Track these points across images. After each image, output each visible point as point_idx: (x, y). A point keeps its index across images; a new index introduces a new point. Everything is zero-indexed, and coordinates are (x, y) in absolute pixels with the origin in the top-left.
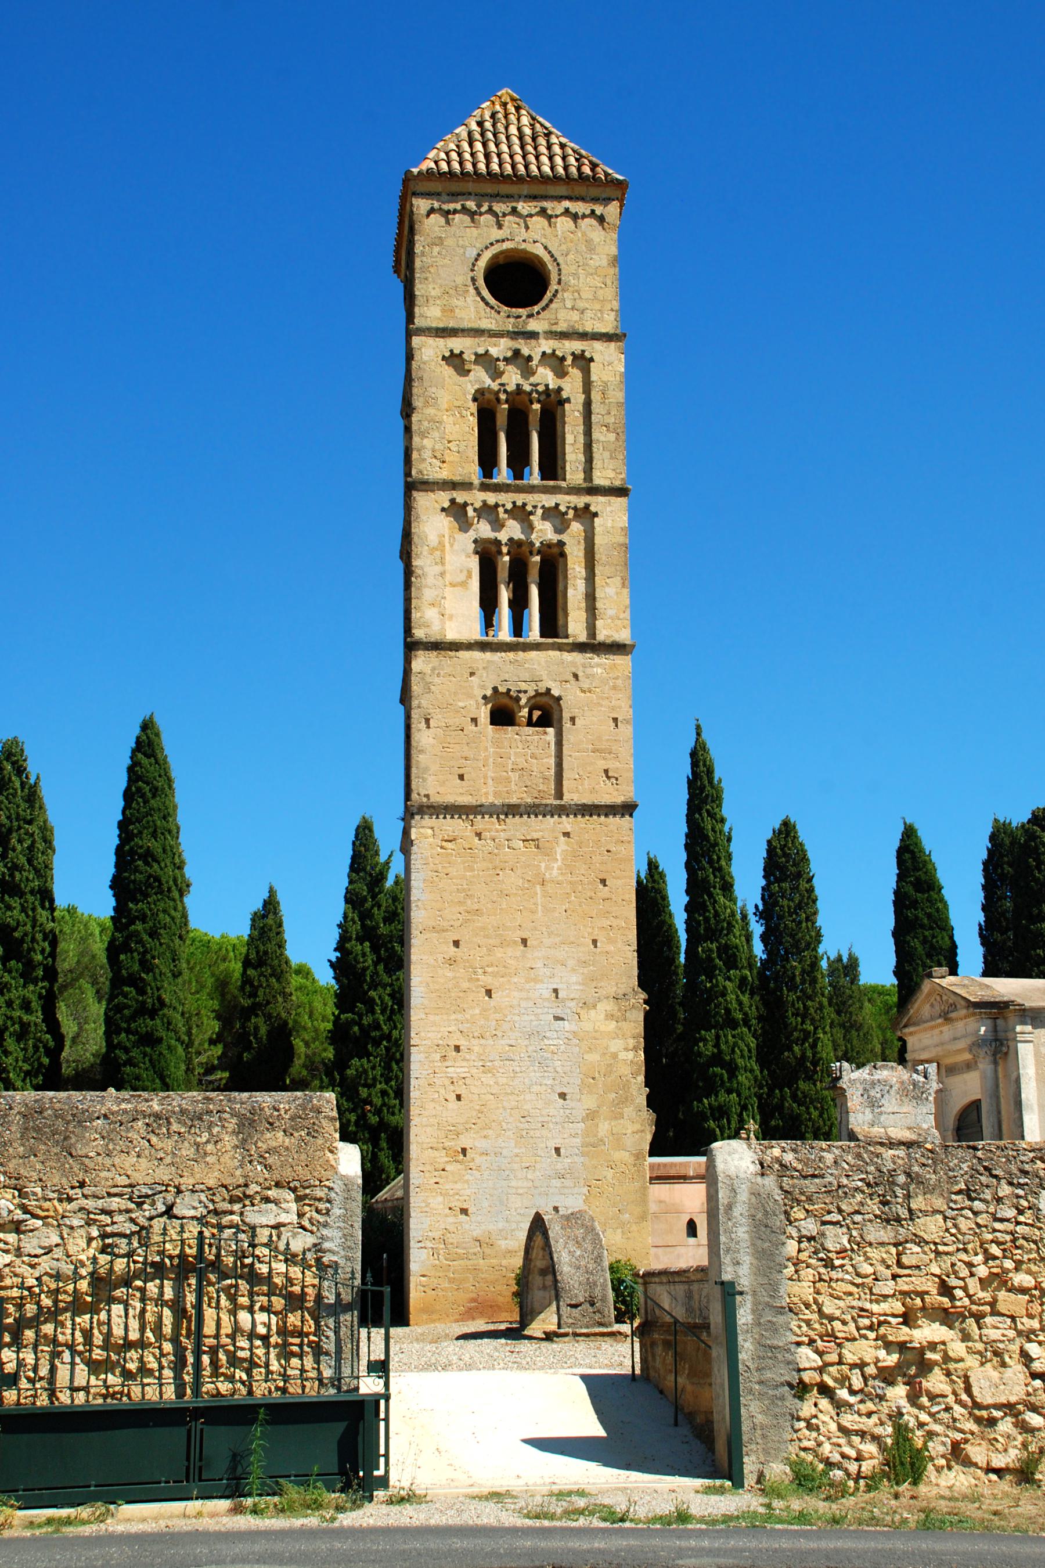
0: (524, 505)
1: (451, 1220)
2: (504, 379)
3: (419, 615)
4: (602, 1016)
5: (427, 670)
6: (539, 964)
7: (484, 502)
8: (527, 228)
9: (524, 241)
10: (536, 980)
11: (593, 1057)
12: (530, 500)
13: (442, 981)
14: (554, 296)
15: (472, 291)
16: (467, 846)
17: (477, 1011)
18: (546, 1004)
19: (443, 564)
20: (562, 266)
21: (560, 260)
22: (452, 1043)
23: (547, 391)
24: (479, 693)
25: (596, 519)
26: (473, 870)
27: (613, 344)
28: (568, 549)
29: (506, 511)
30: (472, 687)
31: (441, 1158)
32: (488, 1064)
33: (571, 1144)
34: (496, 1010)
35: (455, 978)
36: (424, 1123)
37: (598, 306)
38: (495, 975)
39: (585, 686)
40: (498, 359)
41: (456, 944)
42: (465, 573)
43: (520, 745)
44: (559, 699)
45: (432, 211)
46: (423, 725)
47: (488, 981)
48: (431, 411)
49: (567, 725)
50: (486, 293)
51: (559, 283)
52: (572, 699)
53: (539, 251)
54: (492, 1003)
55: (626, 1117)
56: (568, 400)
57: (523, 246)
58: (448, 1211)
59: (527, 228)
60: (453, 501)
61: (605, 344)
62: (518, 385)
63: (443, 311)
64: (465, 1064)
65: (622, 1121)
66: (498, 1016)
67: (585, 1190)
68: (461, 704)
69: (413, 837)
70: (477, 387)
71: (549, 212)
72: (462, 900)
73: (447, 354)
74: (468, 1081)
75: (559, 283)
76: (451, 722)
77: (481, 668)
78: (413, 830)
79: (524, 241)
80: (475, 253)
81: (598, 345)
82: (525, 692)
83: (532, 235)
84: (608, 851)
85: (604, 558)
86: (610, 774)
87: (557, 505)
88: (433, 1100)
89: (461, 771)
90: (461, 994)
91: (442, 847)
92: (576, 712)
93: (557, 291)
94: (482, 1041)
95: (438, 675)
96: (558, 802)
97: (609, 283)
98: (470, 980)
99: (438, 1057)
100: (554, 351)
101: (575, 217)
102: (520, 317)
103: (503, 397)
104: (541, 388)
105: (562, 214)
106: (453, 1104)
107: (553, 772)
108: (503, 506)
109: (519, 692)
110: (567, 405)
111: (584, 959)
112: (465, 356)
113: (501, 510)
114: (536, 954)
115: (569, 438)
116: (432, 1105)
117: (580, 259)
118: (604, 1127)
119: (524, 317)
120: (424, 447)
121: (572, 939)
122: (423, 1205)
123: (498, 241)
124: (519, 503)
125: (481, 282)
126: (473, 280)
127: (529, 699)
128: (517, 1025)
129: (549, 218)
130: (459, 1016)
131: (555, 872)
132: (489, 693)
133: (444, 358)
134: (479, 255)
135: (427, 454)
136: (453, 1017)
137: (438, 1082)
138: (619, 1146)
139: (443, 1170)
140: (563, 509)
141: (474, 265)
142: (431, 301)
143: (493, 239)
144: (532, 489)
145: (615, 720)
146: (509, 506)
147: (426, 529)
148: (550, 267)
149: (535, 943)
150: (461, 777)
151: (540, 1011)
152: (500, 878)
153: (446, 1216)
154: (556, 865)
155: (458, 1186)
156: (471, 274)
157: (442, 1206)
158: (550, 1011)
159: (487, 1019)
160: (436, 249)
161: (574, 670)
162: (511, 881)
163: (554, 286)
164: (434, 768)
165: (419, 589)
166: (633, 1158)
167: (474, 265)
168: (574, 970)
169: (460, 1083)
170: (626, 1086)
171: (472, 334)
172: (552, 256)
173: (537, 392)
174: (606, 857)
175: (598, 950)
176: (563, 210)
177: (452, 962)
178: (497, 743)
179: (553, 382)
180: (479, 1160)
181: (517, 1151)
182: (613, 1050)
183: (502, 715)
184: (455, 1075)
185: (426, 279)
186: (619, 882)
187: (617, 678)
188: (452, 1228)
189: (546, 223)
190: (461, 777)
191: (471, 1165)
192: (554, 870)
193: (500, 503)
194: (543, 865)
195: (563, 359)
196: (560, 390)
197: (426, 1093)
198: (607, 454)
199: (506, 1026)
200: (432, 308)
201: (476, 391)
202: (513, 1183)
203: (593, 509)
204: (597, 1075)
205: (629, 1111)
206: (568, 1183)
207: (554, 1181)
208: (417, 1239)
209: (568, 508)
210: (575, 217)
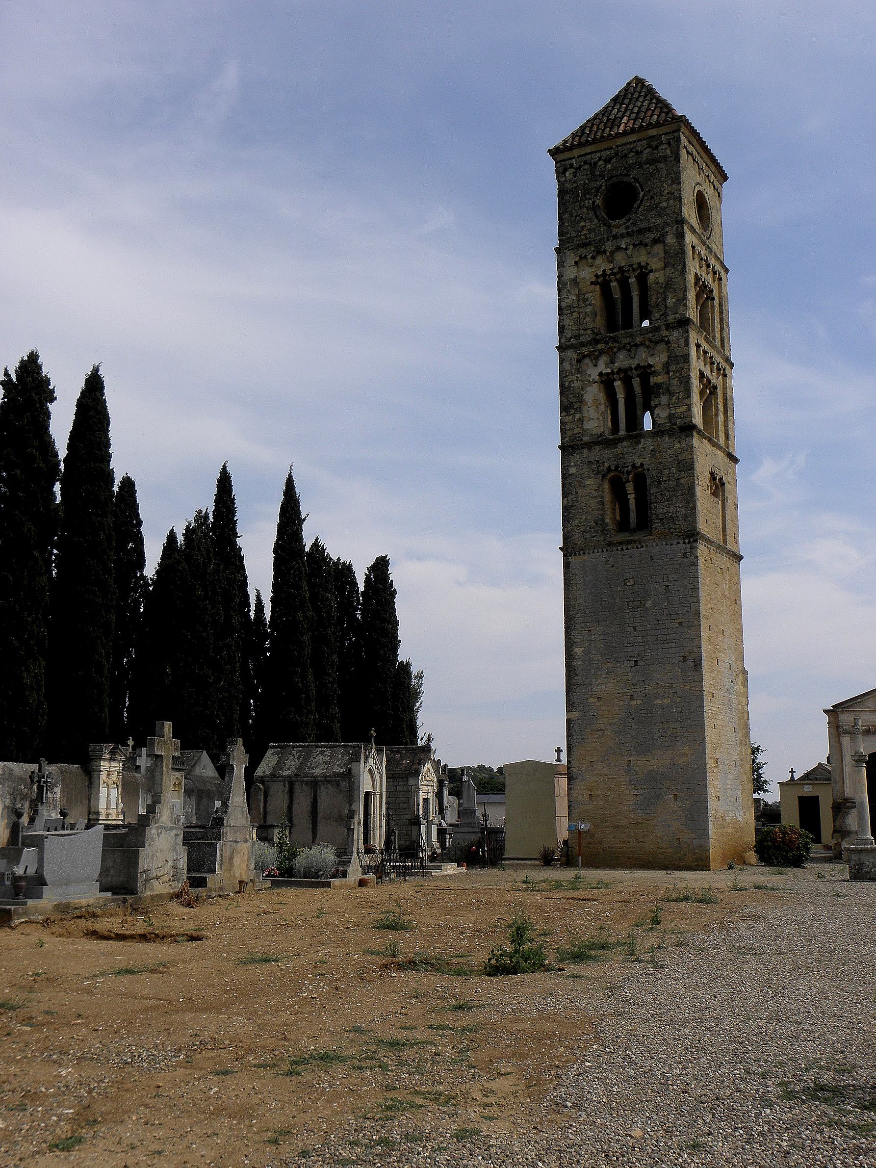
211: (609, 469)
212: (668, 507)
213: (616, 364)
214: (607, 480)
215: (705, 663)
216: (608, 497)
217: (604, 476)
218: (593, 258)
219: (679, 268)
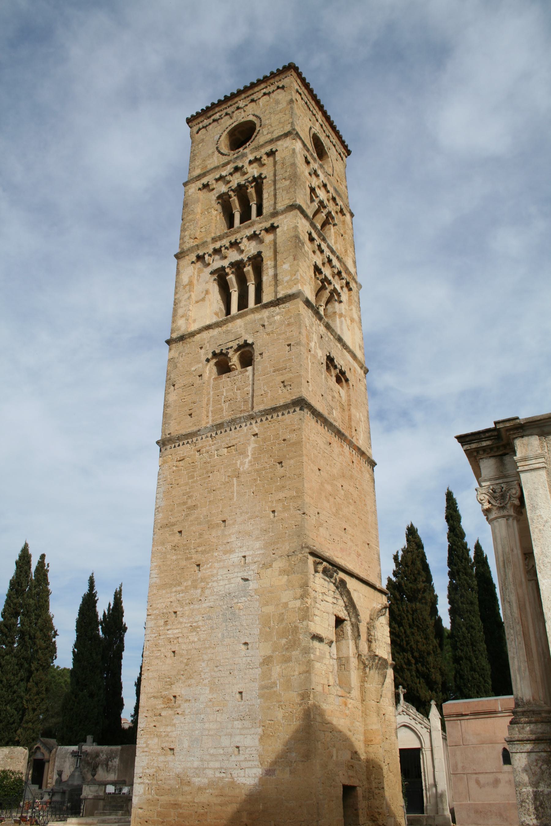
0: (236, 240)
1: (162, 758)
4: (277, 573)
6: (233, 538)
9: (243, 118)
10: (231, 551)
12: (238, 236)
13: (169, 563)
14: (258, 133)
15: (216, 153)
16: (190, 462)
17: (189, 583)
20: (262, 119)
21: (261, 116)
22: (171, 611)
25: (278, 230)
27: (288, 138)
28: (263, 255)
32: (194, 624)
35: (177, 560)
36: (150, 677)
37: (281, 126)
38: (203, 552)
40: (226, 176)
42: (205, 292)
43: (229, 384)
44: (253, 344)
45: (200, 129)
47: (196, 557)
51: (261, 126)
52: (260, 342)
55: (294, 660)
56: (265, 177)
57: (243, 120)
65: (291, 664)
68: (193, 369)
71: (255, 99)
72: (185, 500)
77: (206, 342)
79: (243, 118)
80: (219, 136)
81: (279, 143)
82: (231, 348)
83: (247, 113)
84: (284, 440)
85: (282, 248)
87: (255, 232)
89: (190, 412)
91: (176, 466)
93: (259, 131)
94: (192, 606)
97: (287, 112)
98: (187, 559)
99: (161, 622)
103: (231, 193)
105: (262, 96)
108: (224, 246)
111: (264, 528)
113: (223, 249)
118: (277, 670)
121: (257, 513)
128: (215, 590)
130: (179, 588)
131: (246, 466)
132: (210, 356)
134: (221, 136)
140: (257, 233)
144: (238, 231)
146: (228, 245)
147: (183, 277)
148: (256, 122)
149: (231, 522)
150: (190, 415)
151: (231, 576)
152: (210, 479)
153: (159, 755)
154: (247, 460)
155: (169, 729)
158: (239, 575)
161: (262, 323)
163: (258, 129)
167: (218, 142)
169: (175, 642)
174: (283, 444)
176: (262, 94)
177: (175, 548)
178: (216, 388)
181: (210, 697)
182: (284, 600)
186: (292, 462)
188: (161, 765)
192: (245, 464)
193: (223, 245)
194: (238, 462)
195: (261, 158)
196: (261, 174)
199: (207, 592)
201: (219, 197)
202: (207, 725)
203: (275, 225)
206: (247, 724)
208: (138, 775)
210: (269, 94)
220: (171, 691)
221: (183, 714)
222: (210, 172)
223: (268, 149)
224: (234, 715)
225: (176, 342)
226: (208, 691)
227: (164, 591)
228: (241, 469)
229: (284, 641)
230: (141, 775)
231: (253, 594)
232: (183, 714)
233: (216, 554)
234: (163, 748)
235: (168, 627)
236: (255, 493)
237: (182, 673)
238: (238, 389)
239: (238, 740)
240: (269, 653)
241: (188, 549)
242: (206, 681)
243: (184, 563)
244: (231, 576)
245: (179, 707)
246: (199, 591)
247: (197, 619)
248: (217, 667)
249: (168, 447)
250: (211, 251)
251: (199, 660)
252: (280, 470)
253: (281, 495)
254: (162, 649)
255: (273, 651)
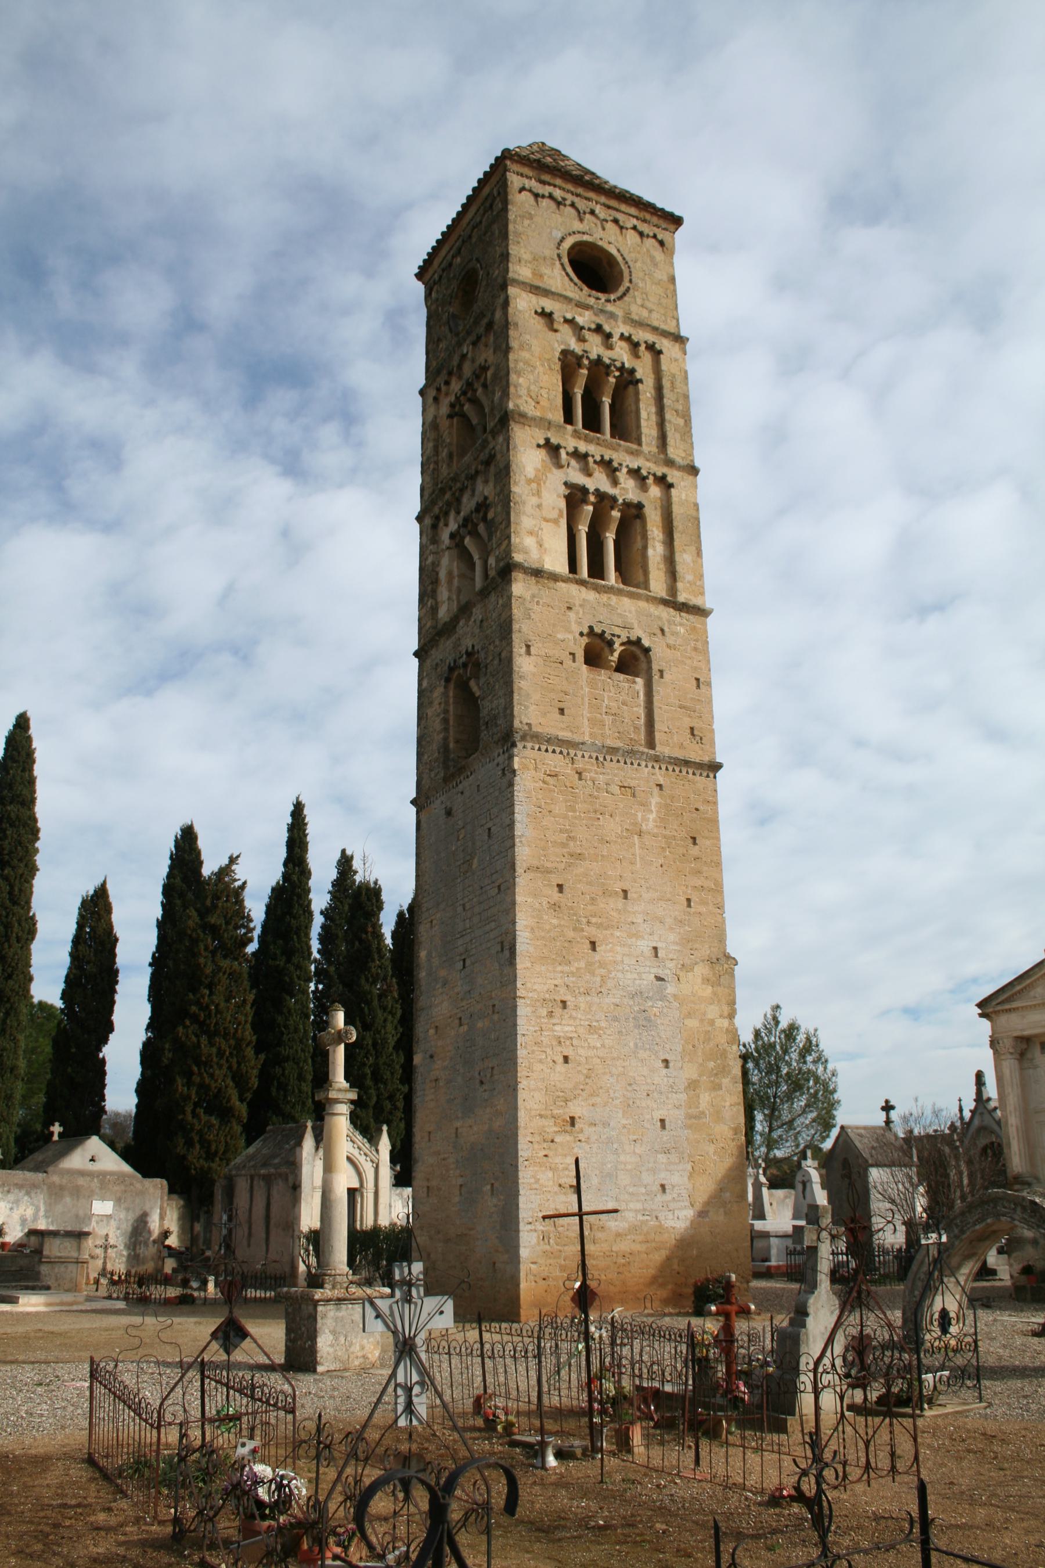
1: (563, 1198)
2: (587, 346)
3: (518, 540)
4: (699, 980)
5: (528, 596)
7: (576, 449)
8: (604, 229)
10: (637, 936)
11: (692, 1023)
13: (548, 927)
17: (582, 964)
18: (648, 963)
19: (540, 497)
20: (632, 270)
21: (630, 263)
22: (558, 998)
23: (622, 369)
24: (576, 629)
25: (672, 490)
26: (574, 811)
29: (595, 462)
30: (569, 622)
31: (551, 1127)
33: (675, 1116)
34: (602, 965)
35: (559, 925)
36: (532, 1087)
38: (599, 926)
39: (671, 642)
41: (560, 887)
45: (522, 189)
46: (523, 650)
47: (592, 932)
48: (525, 355)
49: (656, 677)
50: (569, 270)
53: (613, 251)
54: (597, 957)
56: (640, 381)
57: (600, 243)
58: (557, 1188)
59: (604, 229)
60: (547, 440)
61: (672, 343)
62: (599, 356)
63: (534, 274)
64: (571, 1022)
65: (720, 1093)
66: (603, 971)
67: (689, 1167)
68: (560, 636)
69: (516, 767)
70: (563, 347)
73: (539, 310)
74: (575, 1042)
75: (631, 281)
76: (551, 653)
78: (516, 759)
80: (559, 235)
82: (619, 637)
84: (697, 810)
86: (696, 732)
87: (639, 469)
88: (541, 1061)
89: (561, 705)
90: (566, 945)
91: (544, 782)
92: (663, 665)
93: (629, 288)
94: (589, 998)
95: (538, 603)
96: (652, 752)
99: (544, 1012)
100: (630, 335)
101: (641, 234)
102: (598, 299)
103: (586, 362)
104: (618, 364)
106: (560, 1067)
107: (642, 721)
109: (613, 635)
110: (640, 385)
112: (555, 316)
114: (636, 908)
115: (644, 414)
116: (541, 1066)
117: (645, 268)
118: (705, 1099)
119: (603, 300)
120: (520, 385)
121: (669, 896)
122: (532, 1181)
123: (579, 232)
124: (607, 458)
125: (565, 260)
126: (559, 256)
127: (622, 644)
129: (621, 228)
130: (566, 969)
131: (651, 824)
132: (586, 631)
133: (536, 312)
135: (523, 392)
136: (559, 968)
137: (545, 1040)
138: (718, 1116)
139: (552, 1141)
140: (644, 472)
141: (559, 245)
142: (523, 262)
143: (575, 229)
145: (697, 680)
146: (598, 458)
147: (523, 460)
149: (635, 896)
150: (562, 711)
151: (642, 969)
156: (557, 251)
157: (551, 1183)
158: (653, 970)
159: (593, 974)
160: (526, 222)
162: (612, 827)
163: (626, 284)
164: (536, 697)
165: (518, 514)
166: (731, 1132)
167: (559, 245)
168: (672, 929)
170: (724, 1054)
171: (561, 299)
172: (624, 259)
173: (615, 366)
175: (692, 910)
177: (555, 907)
178: (592, 684)
179: (628, 362)
180: (589, 1131)
181: (624, 1122)
182: (710, 1016)
183: (593, 658)
184: (562, 1034)
185: (519, 243)
187: (697, 640)
189: (618, 231)
190: (562, 711)
191: (581, 1137)
192: (650, 820)
194: (640, 815)
197: (533, 1052)
198: (678, 436)
199: (610, 984)
200: (524, 268)
202: (622, 1158)
204: (696, 1043)
205: (726, 1081)
206: (674, 1157)
207: (659, 1156)
209: (649, 473)
210: (641, 234)
211: (451, 669)
212: (491, 702)
213: (462, 514)
214: (452, 685)
215: (520, 948)
216: (451, 708)
217: (448, 680)
218: (447, 383)
219: (504, 346)
220: (567, 1110)
221: (588, 1140)
222: (556, 298)
223: (651, 338)
224: (656, 1147)
225: (525, 573)
226: (620, 1115)
227: (543, 968)
228: (644, 827)
229: (711, 1064)
230: (530, 1220)
231: (672, 1000)
232: (588, 1140)
233: (618, 934)
234: (560, 1185)
235: (554, 1021)
236: (665, 867)
237: (582, 1087)
238: (624, 703)
239: (663, 1177)
240: (695, 1076)
241: (575, 915)
242: (617, 1102)
243: (571, 934)
244: (642, 969)
245: (582, 1131)
246: (598, 979)
247: (597, 1017)
248: (630, 1085)
249: (529, 745)
250: (571, 450)
251: (604, 1073)
252: (694, 851)
253: (699, 882)
254: (549, 1050)
255: (700, 1076)
